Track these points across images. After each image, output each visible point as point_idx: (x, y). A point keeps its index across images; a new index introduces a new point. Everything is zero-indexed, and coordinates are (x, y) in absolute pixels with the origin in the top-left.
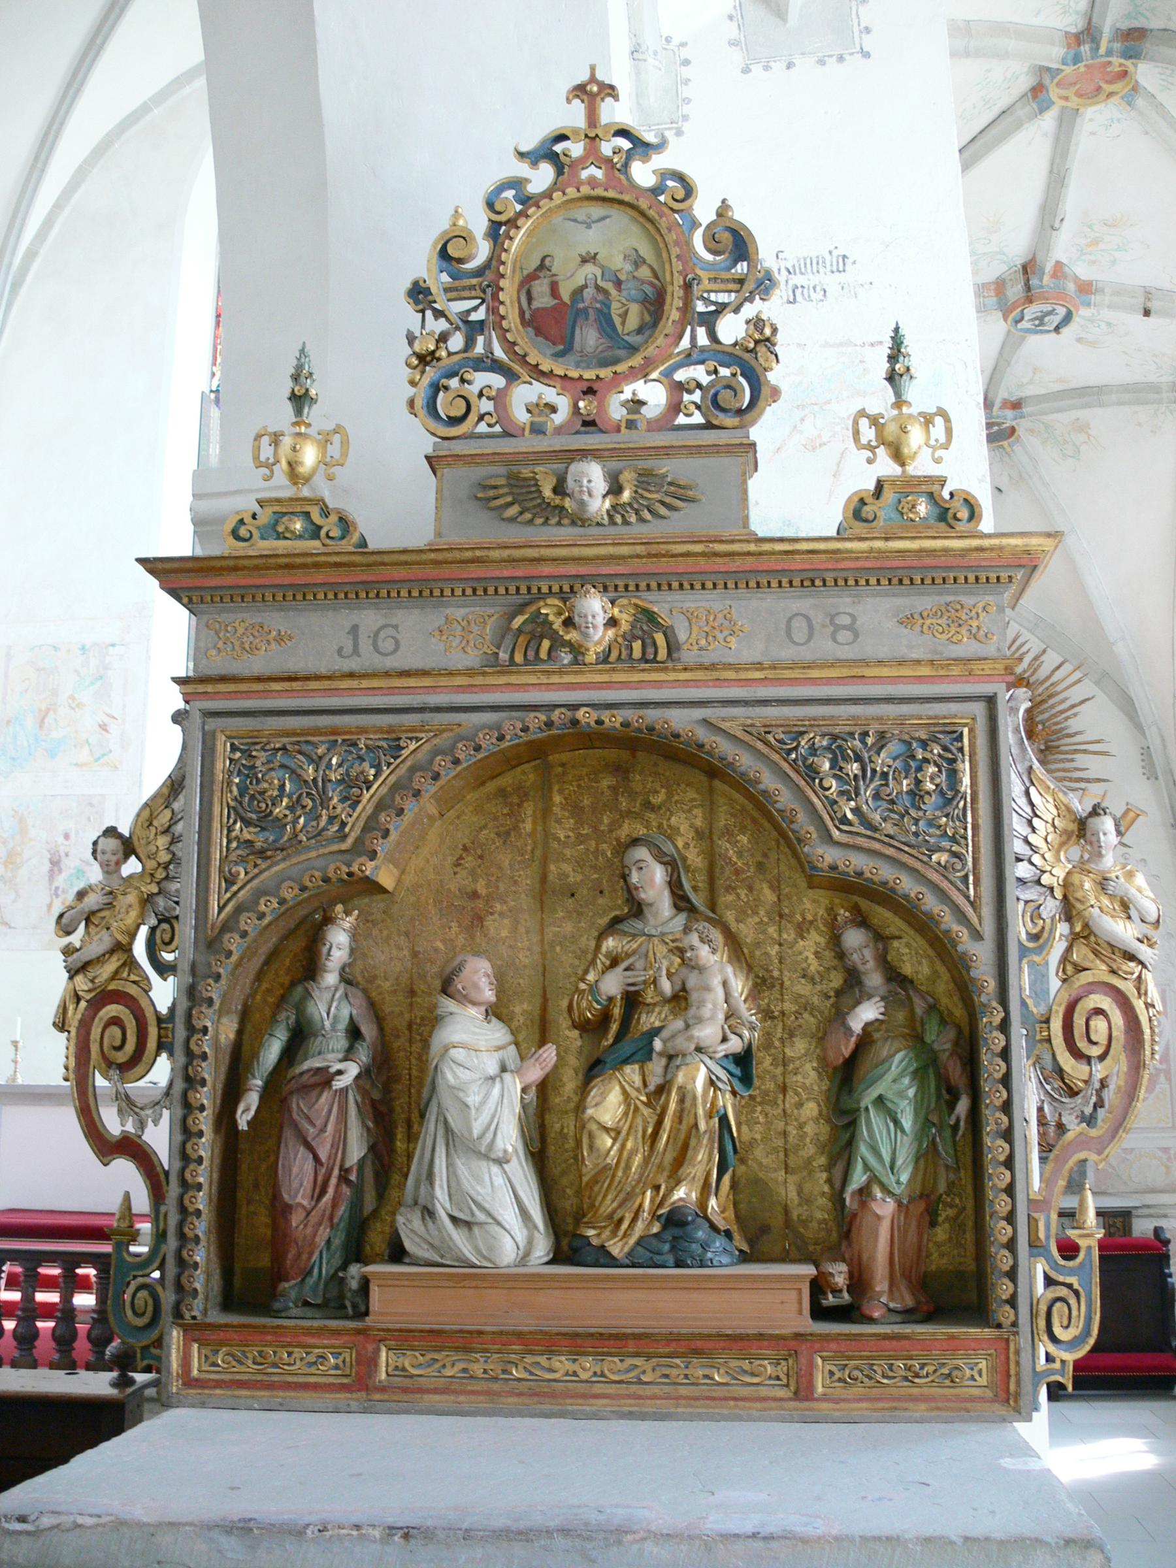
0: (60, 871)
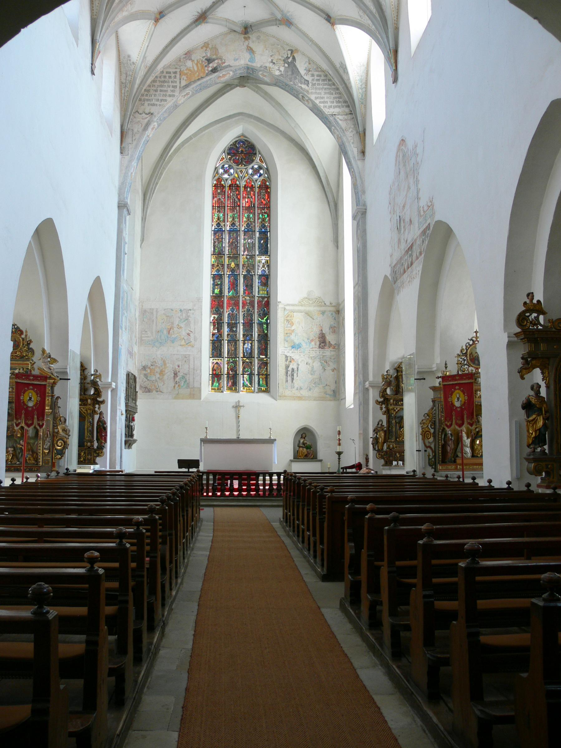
0: (177, 376)
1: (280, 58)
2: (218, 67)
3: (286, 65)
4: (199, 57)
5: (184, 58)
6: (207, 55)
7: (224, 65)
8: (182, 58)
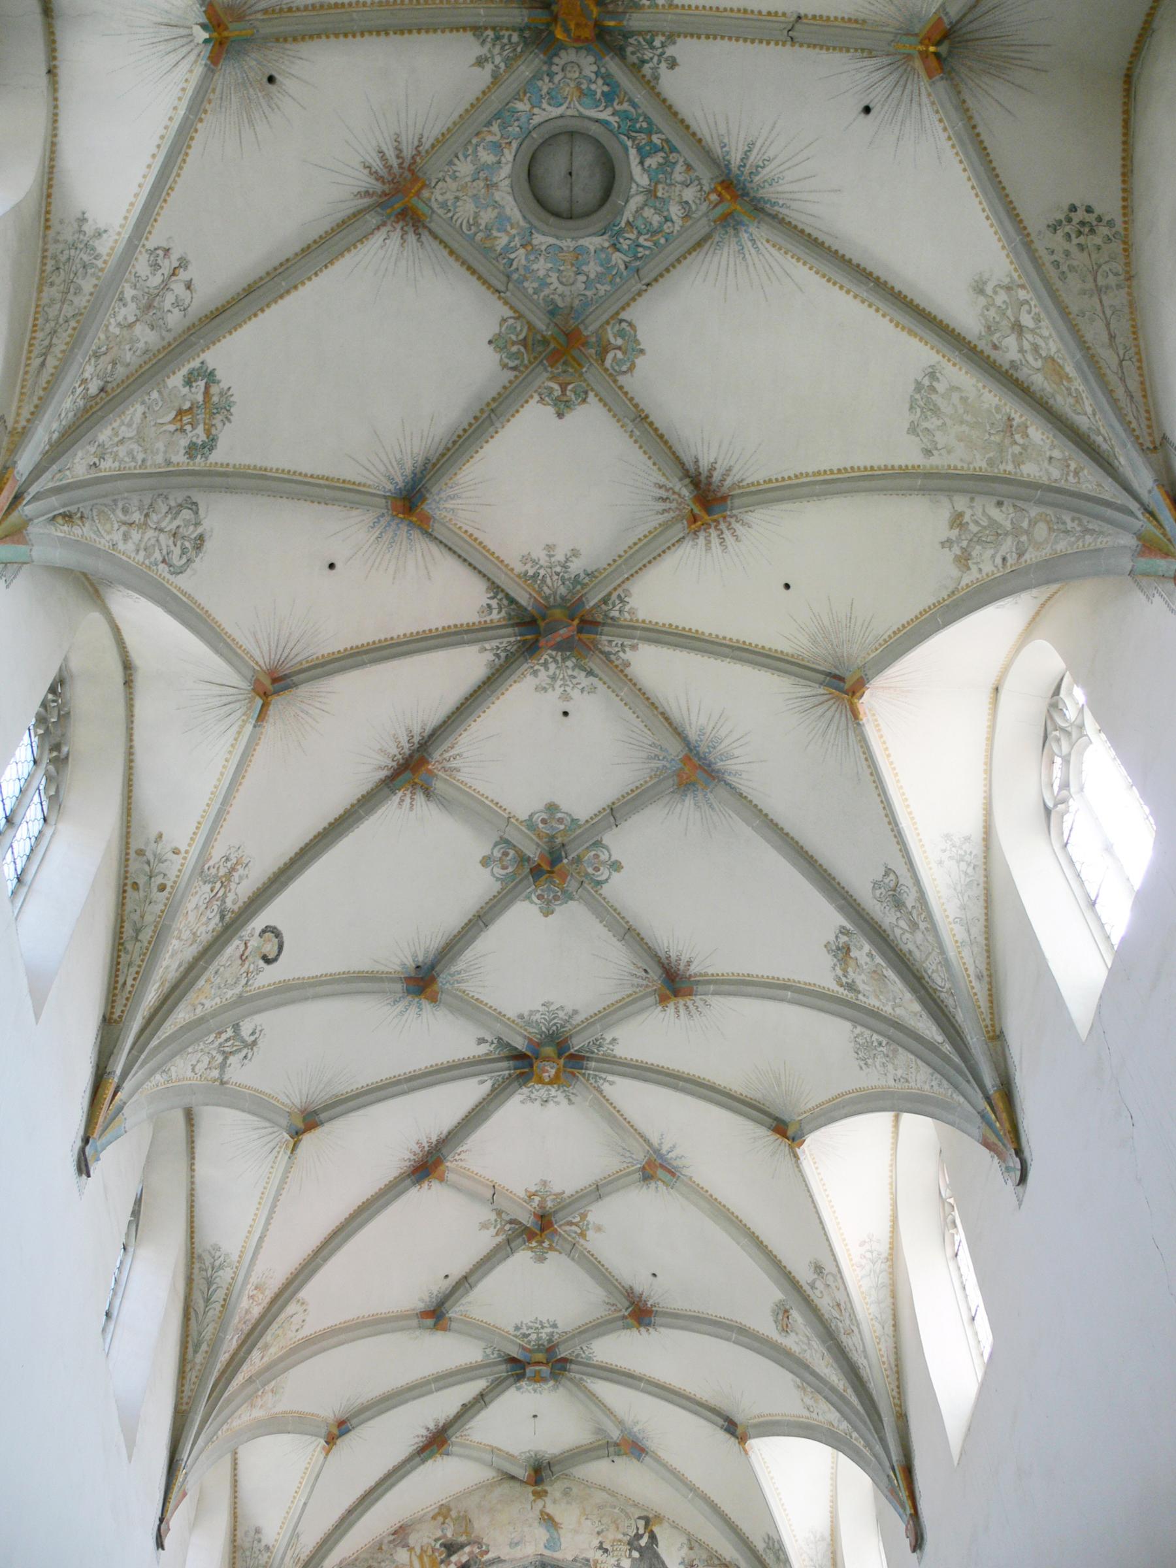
1: (620, 1536)
2: (472, 1562)
3: (636, 1554)
4: (426, 1541)
5: (390, 1542)
6: (445, 1536)
7: (486, 1557)
8: (386, 1541)
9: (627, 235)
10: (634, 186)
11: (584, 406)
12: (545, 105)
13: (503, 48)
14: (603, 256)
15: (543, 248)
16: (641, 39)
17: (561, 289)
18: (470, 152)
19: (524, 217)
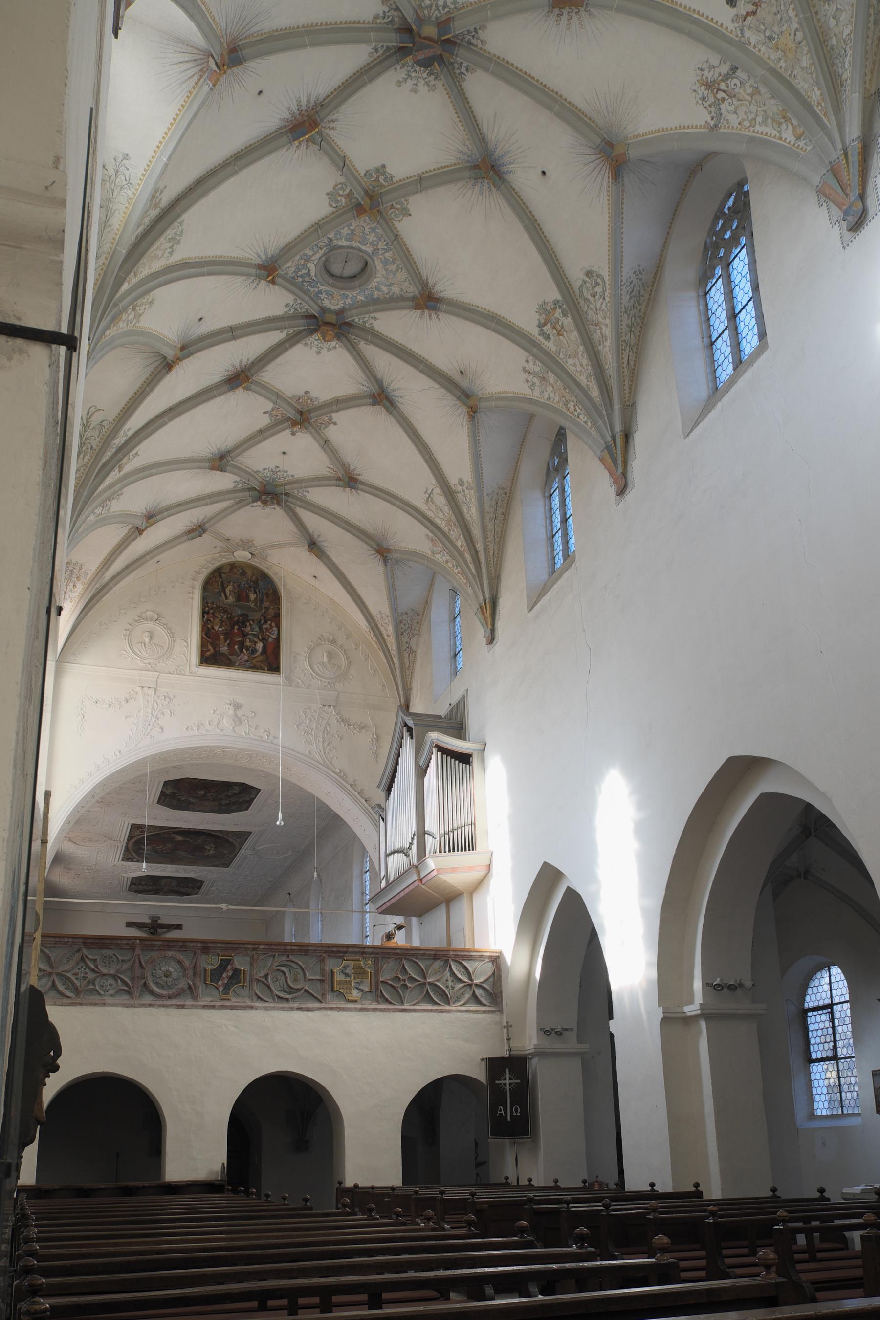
9: (324, 244)
10: (315, 263)
11: (367, 169)
12: (350, 296)
13: (363, 318)
14: (338, 236)
15: (368, 245)
16: (300, 311)
17: (365, 225)
18: (391, 295)
19: (373, 261)
